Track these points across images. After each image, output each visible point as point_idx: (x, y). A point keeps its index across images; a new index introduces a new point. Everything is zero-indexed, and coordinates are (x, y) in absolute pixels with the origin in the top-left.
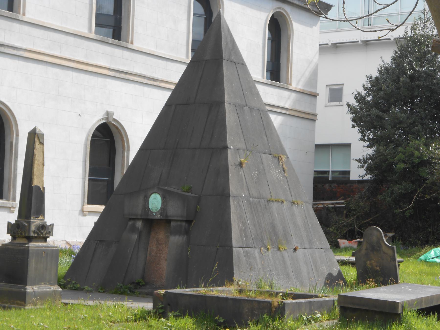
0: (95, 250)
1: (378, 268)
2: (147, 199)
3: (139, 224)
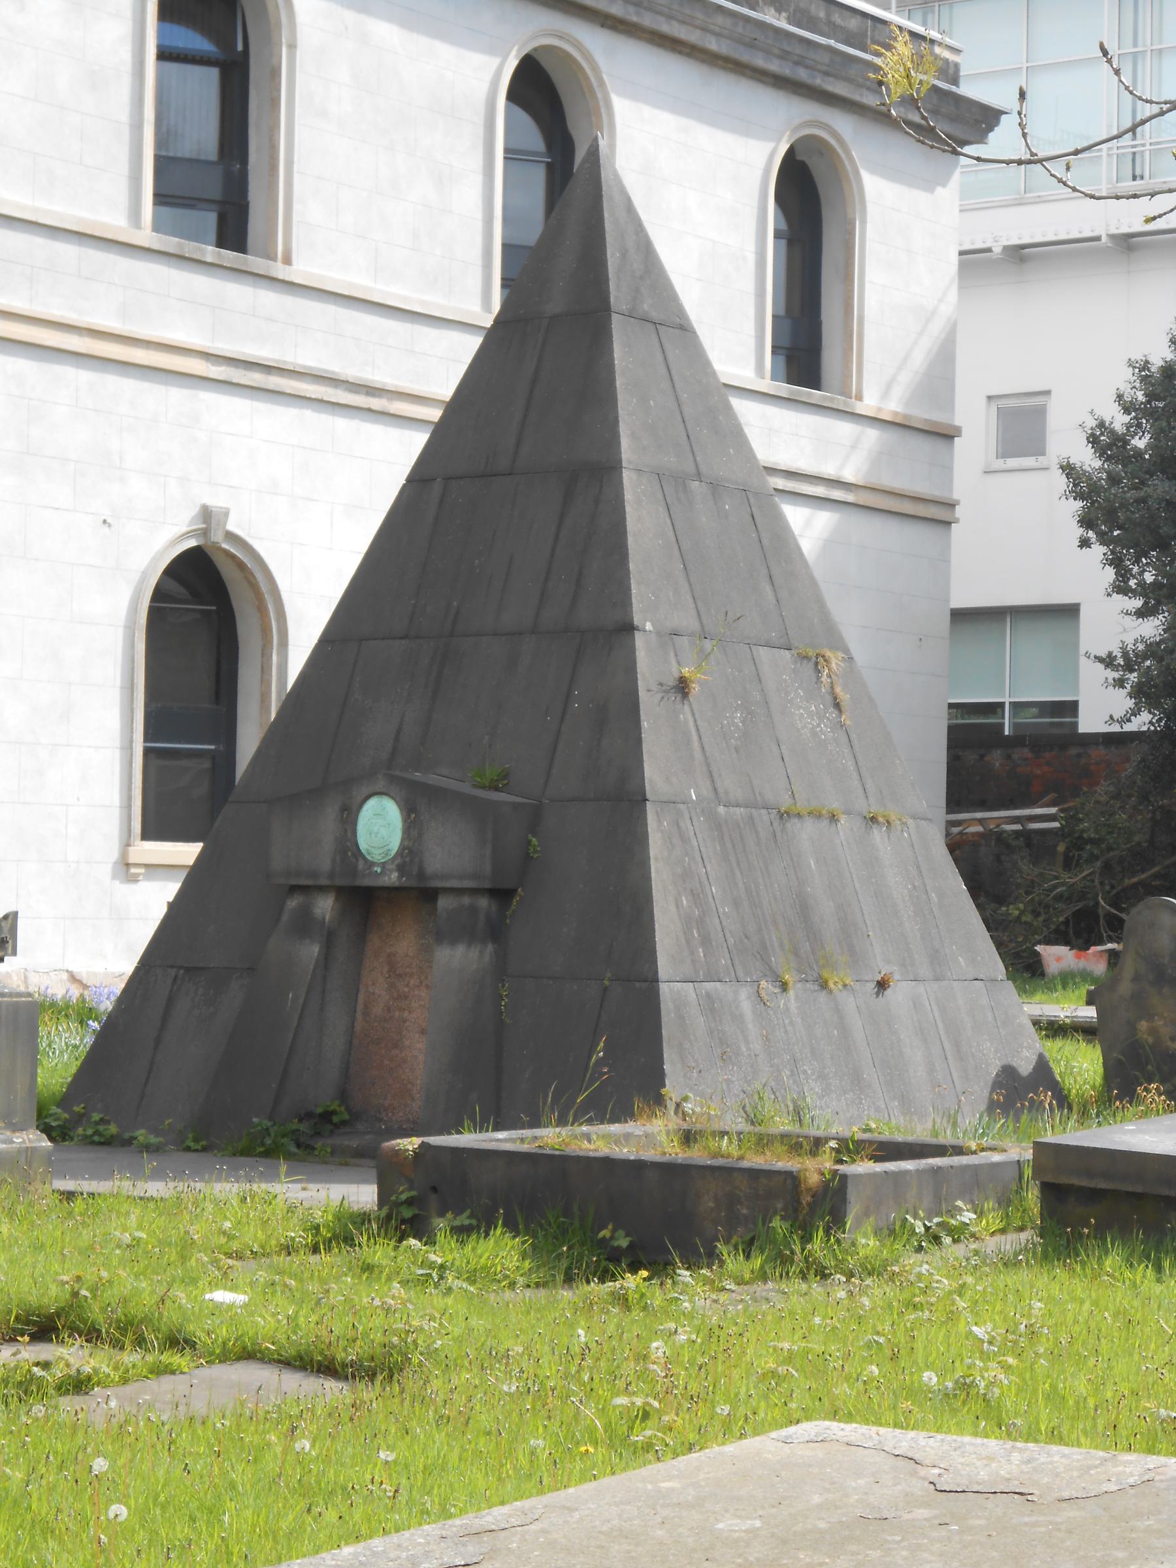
0: (170, 1001)
2: (349, 816)
3: (325, 906)
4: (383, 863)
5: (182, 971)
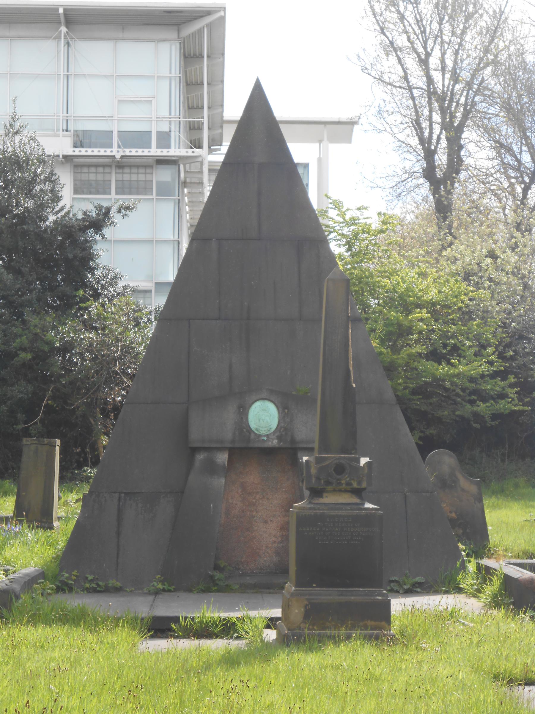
0: (120, 512)
1: (453, 515)
2: (243, 411)
3: (223, 458)
4: (267, 435)
5: (123, 495)
